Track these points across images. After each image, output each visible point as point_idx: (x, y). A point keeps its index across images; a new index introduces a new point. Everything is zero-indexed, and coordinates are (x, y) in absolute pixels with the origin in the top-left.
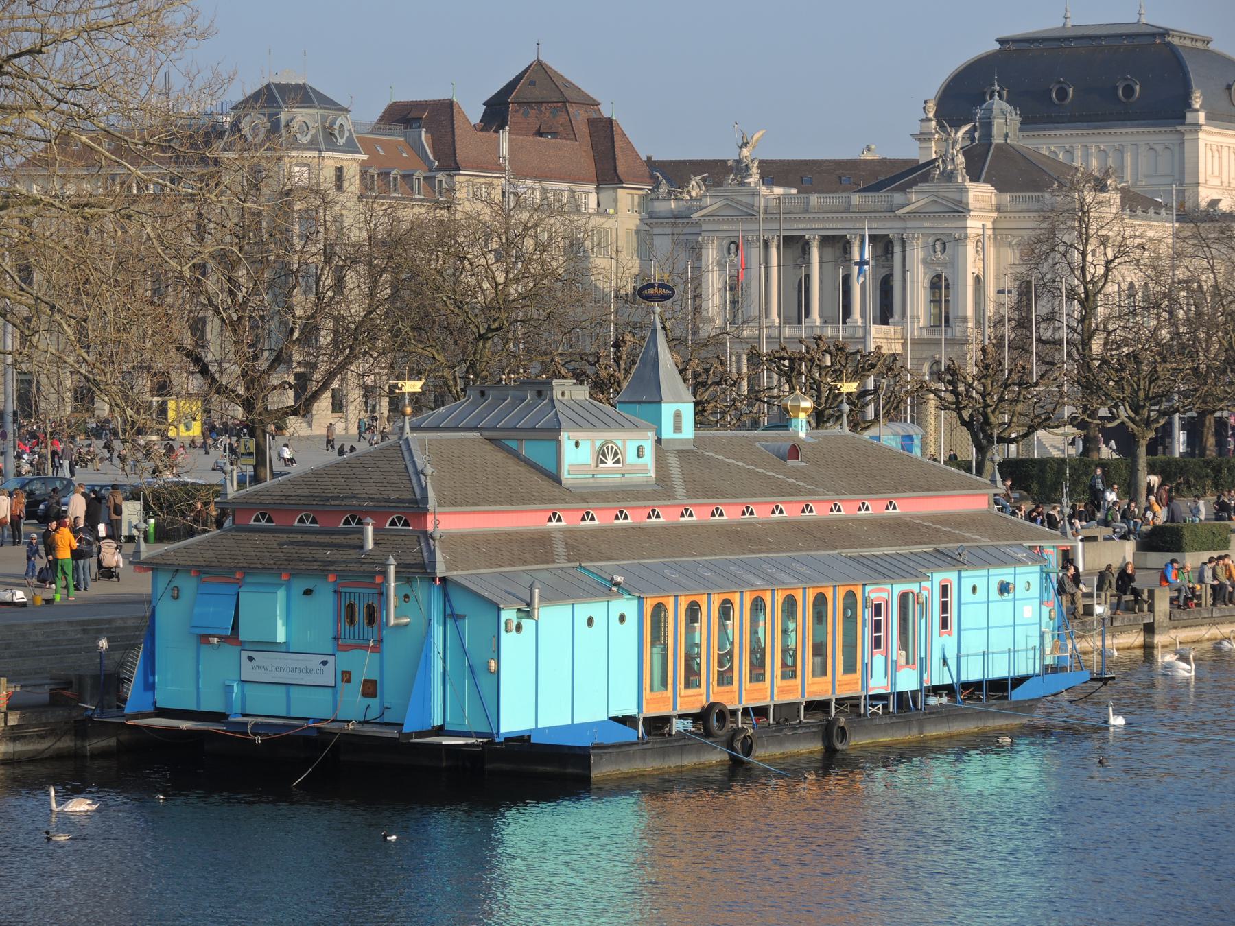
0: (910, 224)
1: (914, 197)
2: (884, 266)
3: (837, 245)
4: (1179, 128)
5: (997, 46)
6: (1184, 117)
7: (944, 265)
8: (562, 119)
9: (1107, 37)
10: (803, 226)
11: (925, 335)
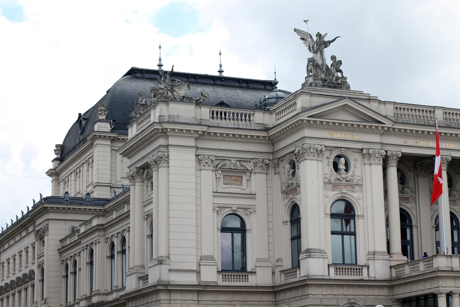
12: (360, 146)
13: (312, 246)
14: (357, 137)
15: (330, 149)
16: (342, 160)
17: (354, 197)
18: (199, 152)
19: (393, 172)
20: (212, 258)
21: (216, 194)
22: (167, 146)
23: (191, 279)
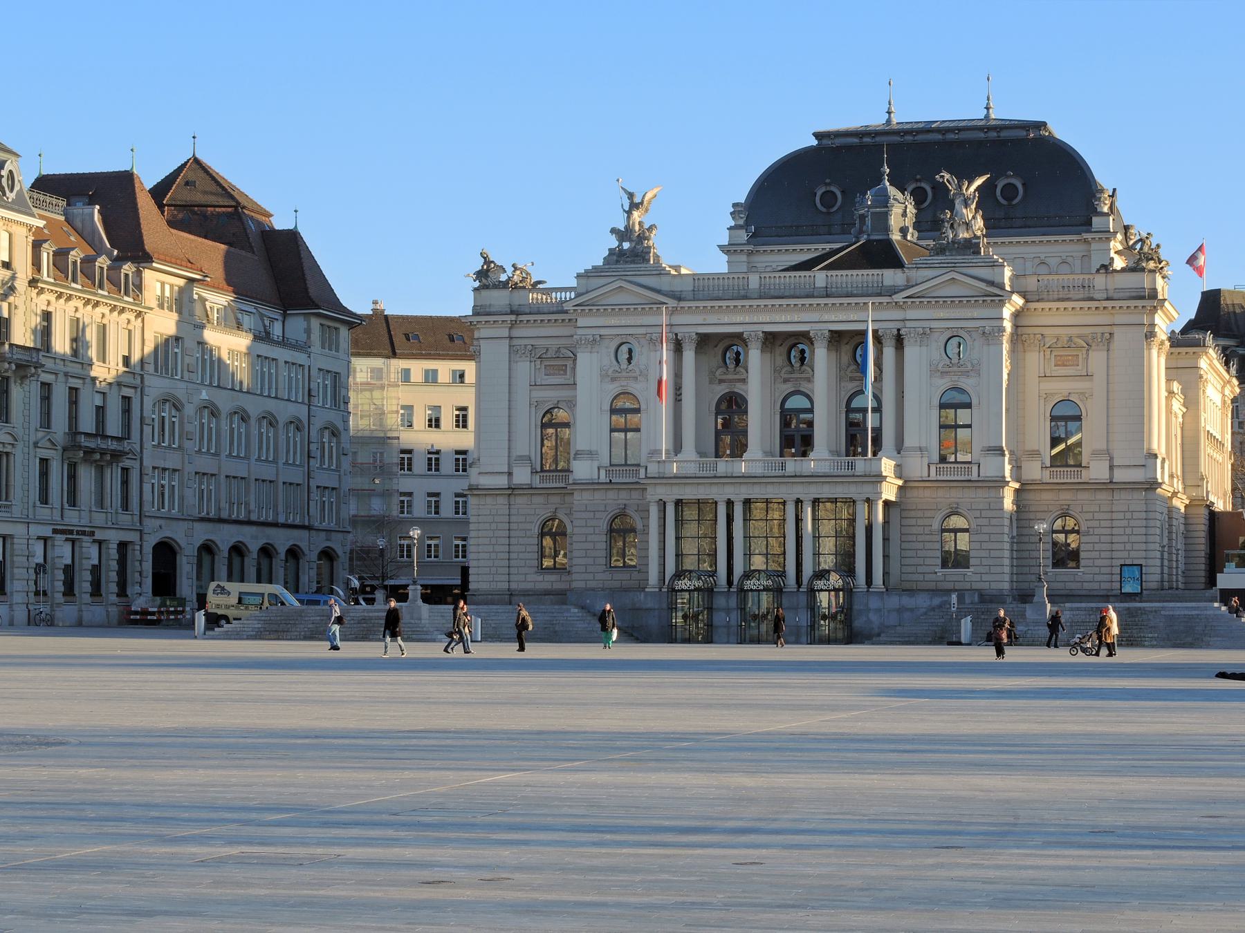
0: (911, 314)
5: (814, 142)
6: (1089, 223)
7: (966, 374)
10: (739, 319)
11: (933, 476)
13: (579, 447)
16: (624, 348)
17: (634, 388)
18: (515, 342)
19: (689, 355)
23: (502, 481)
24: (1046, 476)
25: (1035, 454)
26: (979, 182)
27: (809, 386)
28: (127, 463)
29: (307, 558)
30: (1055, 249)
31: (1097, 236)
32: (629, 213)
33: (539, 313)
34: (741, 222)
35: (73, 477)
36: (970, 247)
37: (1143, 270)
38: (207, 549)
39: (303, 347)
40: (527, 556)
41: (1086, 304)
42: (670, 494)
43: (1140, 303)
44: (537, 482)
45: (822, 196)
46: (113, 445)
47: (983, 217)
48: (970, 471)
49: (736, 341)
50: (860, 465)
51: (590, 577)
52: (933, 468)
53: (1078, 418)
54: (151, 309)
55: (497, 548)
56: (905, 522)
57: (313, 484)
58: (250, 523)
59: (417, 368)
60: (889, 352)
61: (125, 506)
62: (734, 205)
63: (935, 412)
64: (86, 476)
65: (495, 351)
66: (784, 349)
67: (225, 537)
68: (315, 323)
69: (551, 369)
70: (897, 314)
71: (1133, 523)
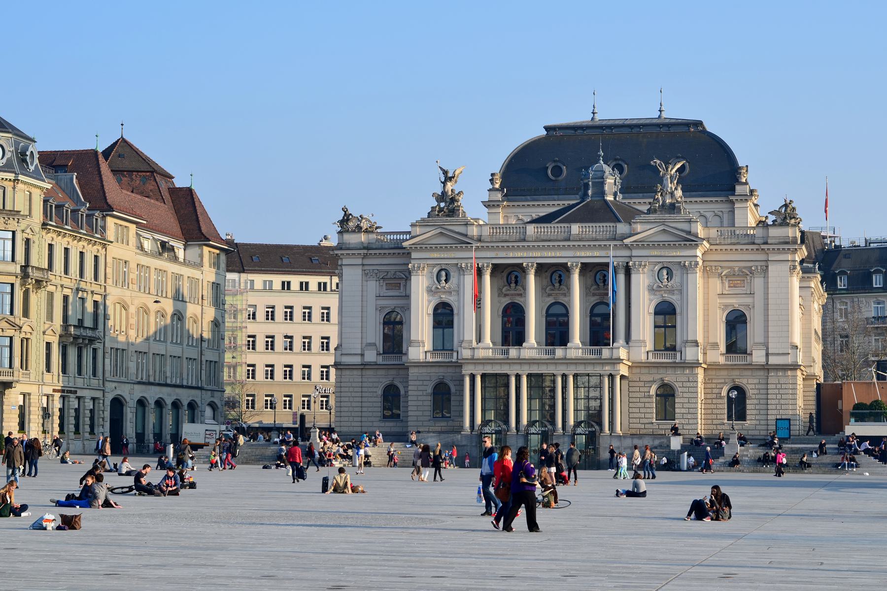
0: (635, 252)
1: (639, 227)
2: (594, 295)
3: (554, 275)
4: (731, 198)
6: (734, 190)
7: (671, 292)
8: (150, 186)
9: (644, 125)
10: (519, 254)
11: (651, 359)
12: (455, 262)
14: (452, 255)
15: (434, 266)
16: (443, 273)
17: (451, 299)
18: (366, 268)
19: (487, 278)
20: (375, 344)
21: (378, 296)
22: (341, 265)
23: (357, 360)
24: (722, 360)
25: (715, 345)
26: (678, 166)
27: (566, 299)
28: (97, 345)
29: (200, 409)
30: (710, 206)
31: (739, 198)
32: (444, 183)
33: (382, 248)
34: (497, 186)
35: (80, 357)
36: (673, 208)
37: (788, 225)
38: (141, 403)
39: (199, 265)
40: (376, 409)
41: (750, 247)
42: (478, 371)
43: (786, 247)
44: (380, 360)
45: (547, 168)
46: (90, 333)
47: (682, 189)
48: (675, 357)
49: (516, 269)
50: (606, 352)
51: (420, 424)
52: (650, 355)
53: (745, 322)
54: (112, 242)
55: (354, 404)
56: (631, 389)
57: (204, 359)
58: (166, 385)
59: (259, 279)
60: (621, 277)
61: (94, 374)
62: (493, 175)
63: (652, 316)
64: (72, 353)
65: (352, 274)
66: (548, 274)
67: (152, 394)
68: (206, 250)
69: (390, 286)
70: (626, 253)
71: (781, 391)
